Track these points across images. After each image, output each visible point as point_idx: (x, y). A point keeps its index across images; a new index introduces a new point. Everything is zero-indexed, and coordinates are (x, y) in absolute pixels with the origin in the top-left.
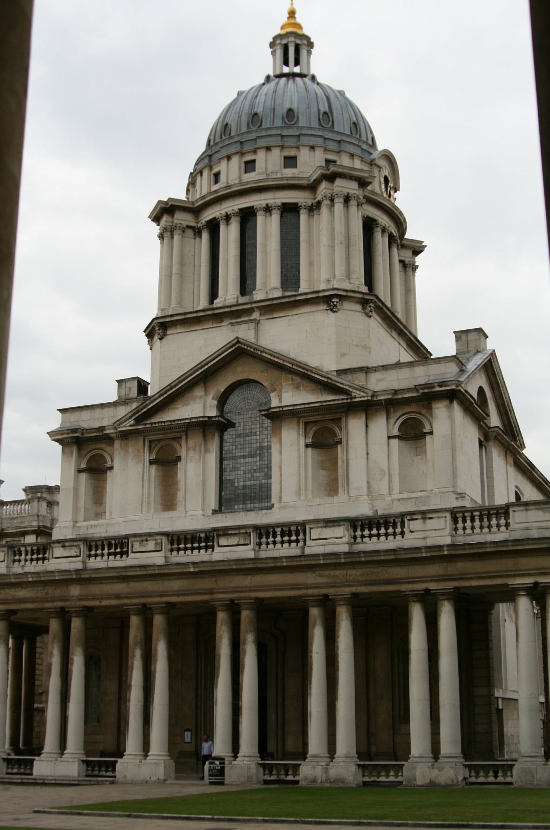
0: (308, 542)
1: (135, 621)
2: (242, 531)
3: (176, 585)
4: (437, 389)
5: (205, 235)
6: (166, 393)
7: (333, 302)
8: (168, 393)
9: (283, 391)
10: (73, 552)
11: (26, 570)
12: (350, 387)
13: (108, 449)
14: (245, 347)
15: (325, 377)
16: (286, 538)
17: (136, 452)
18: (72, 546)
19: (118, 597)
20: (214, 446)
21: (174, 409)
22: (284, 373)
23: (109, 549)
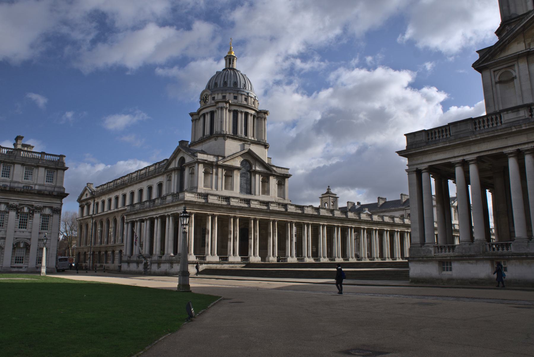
4: (288, 176)
5: (232, 113)
9: (257, 165)
10: (237, 201)
16: (282, 207)
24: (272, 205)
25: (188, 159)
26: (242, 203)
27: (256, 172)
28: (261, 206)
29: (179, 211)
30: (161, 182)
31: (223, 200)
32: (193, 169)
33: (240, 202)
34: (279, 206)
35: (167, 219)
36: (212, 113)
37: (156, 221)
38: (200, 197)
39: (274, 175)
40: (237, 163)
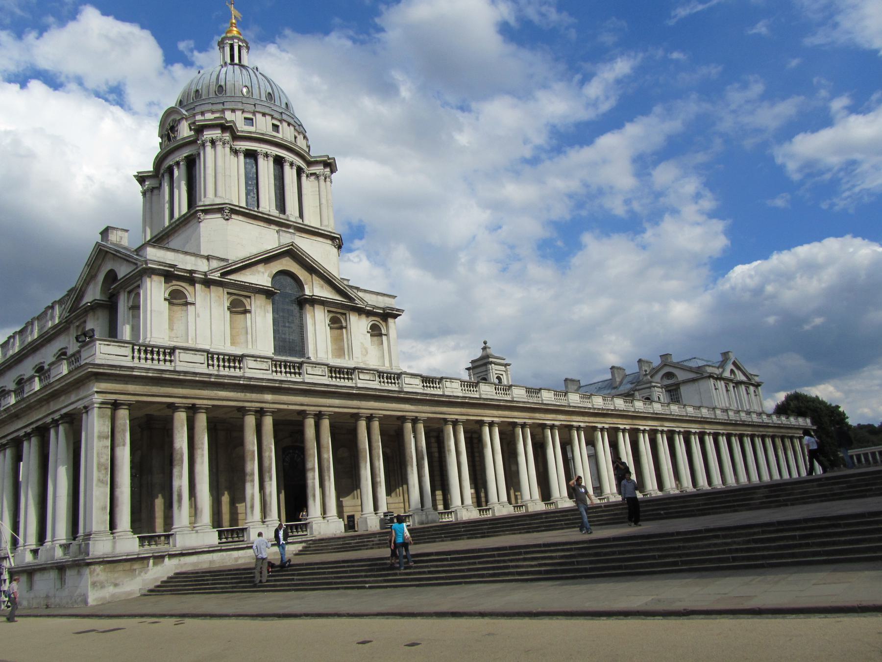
0: (404, 385)
1: (310, 423)
2: (371, 372)
3: (337, 402)
5: (241, 157)
6: (244, 262)
7: (337, 242)
8: (246, 263)
11: (221, 373)
12: (355, 296)
13: (190, 288)
14: (296, 250)
15: (342, 286)
16: (389, 381)
17: (217, 298)
18: (262, 361)
19: (302, 405)
20: (270, 308)
21: (244, 274)
22: (314, 276)
23: (285, 368)
24: (362, 376)
25: (123, 271)
26: (281, 372)
27: (314, 301)
28: (334, 379)
29: (80, 402)
30: (64, 351)
31: (221, 364)
32: (138, 294)
33: (274, 369)
34: (382, 380)
35: (52, 432)
36: (191, 163)
37: (26, 444)
38: (149, 356)
39: (361, 311)
40: (262, 277)
